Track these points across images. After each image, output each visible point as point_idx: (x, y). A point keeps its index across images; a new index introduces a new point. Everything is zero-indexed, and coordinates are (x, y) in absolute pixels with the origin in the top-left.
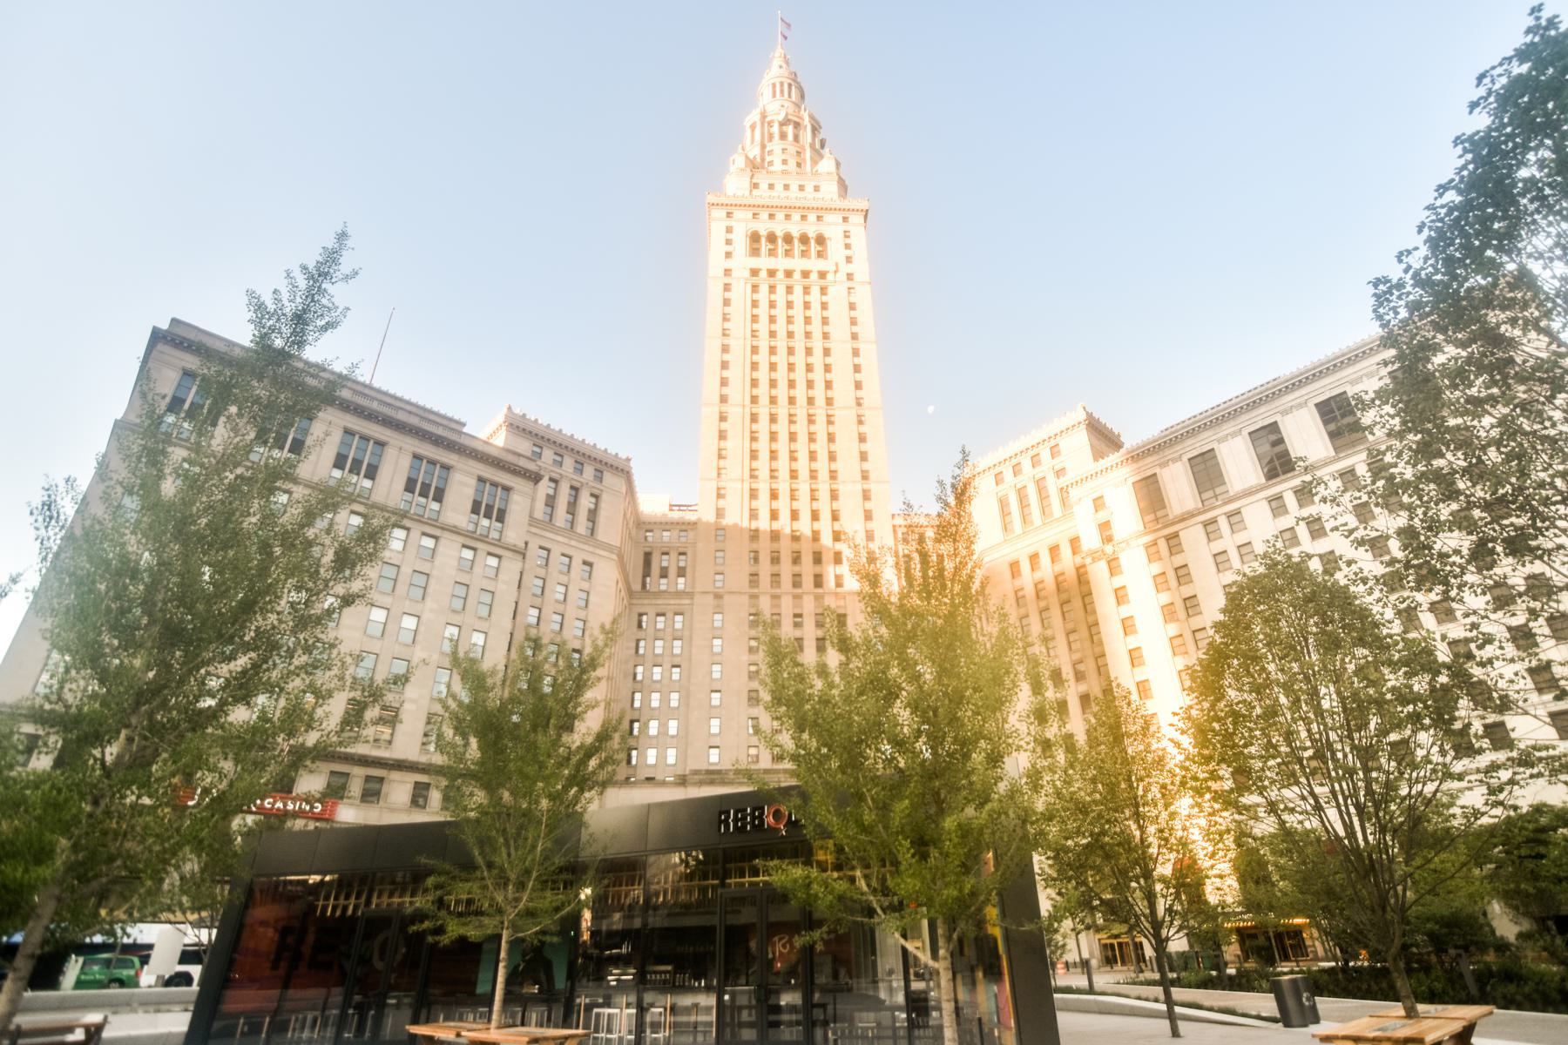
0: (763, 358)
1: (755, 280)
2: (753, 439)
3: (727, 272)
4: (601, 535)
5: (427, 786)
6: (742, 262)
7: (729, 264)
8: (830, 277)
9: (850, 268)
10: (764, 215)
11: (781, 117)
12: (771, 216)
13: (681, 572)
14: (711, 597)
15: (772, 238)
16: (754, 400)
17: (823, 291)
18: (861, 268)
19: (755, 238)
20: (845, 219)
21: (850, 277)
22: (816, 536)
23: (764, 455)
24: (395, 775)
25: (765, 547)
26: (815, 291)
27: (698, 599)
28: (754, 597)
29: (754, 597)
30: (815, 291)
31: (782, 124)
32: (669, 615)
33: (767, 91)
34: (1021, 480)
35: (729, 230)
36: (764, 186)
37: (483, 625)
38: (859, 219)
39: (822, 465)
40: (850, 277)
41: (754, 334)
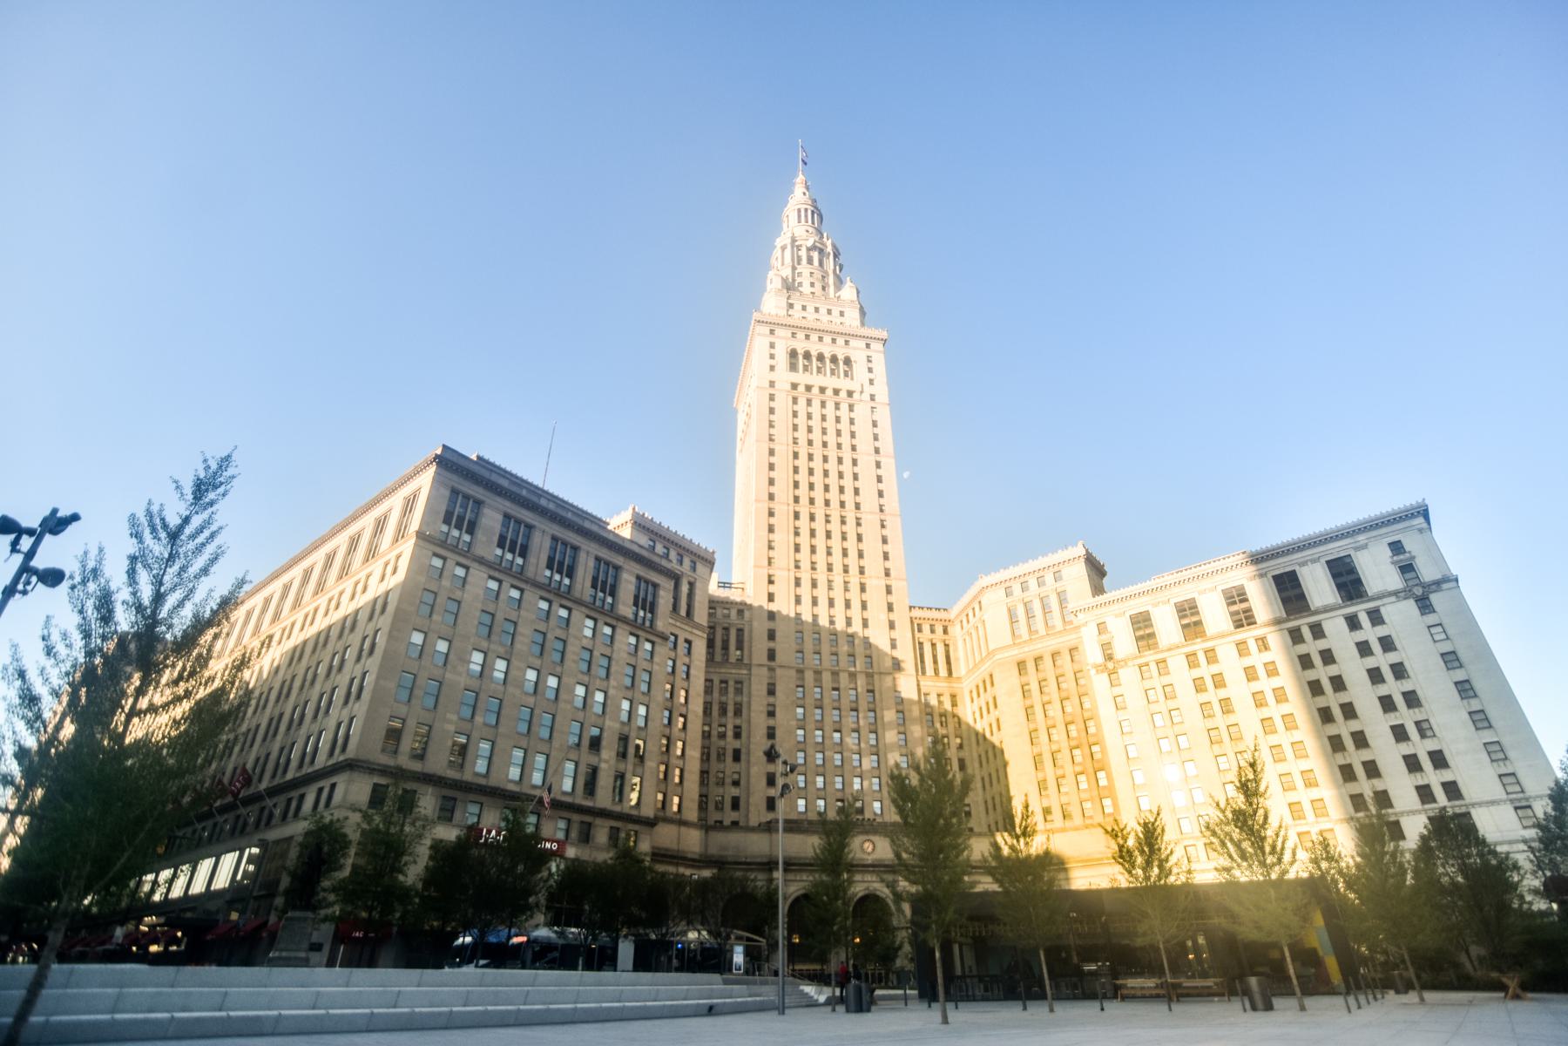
0: (802, 462)
1: (795, 393)
2: (797, 534)
3: (772, 384)
4: (697, 619)
5: (618, 829)
6: (784, 377)
8: (856, 396)
9: (872, 389)
10: (801, 335)
11: (810, 243)
12: (807, 337)
14: (764, 671)
15: (807, 356)
18: (882, 391)
19: (793, 354)
20: (868, 346)
21: (872, 398)
22: (849, 622)
23: (805, 549)
24: (598, 821)
26: (844, 407)
27: (754, 670)
28: (800, 671)
29: (800, 671)
30: (844, 407)
31: (809, 249)
32: (731, 683)
33: (793, 216)
34: (1028, 596)
35: (772, 346)
36: (798, 307)
37: (646, 700)
39: (852, 560)
40: (872, 398)
41: (795, 441)
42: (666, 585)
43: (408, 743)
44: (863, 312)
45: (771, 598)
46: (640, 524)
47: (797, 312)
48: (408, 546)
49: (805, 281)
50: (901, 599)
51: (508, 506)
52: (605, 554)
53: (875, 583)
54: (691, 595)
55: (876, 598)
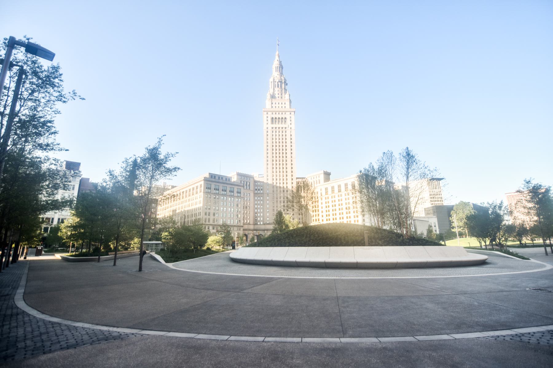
3: (267, 128)
6: (270, 126)
7: (267, 126)
13: (262, 190)
16: (273, 157)
17: (286, 131)
18: (293, 126)
19: (272, 118)
23: (275, 168)
25: (275, 189)
26: (284, 132)
30: (284, 132)
35: (267, 117)
36: (274, 103)
38: (293, 113)
39: (285, 170)
42: (242, 188)
43: (207, 221)
44: (290, 102)
45: (267, 179)
46: (239, 174)
47: (274, 105)
48: (202, 194)
49: (276, 92)
50: (294, 178)
51: (214, 183)
52: (231, 186)
53: (289, 174)
54: (249, 185)
55: (289, 178)
